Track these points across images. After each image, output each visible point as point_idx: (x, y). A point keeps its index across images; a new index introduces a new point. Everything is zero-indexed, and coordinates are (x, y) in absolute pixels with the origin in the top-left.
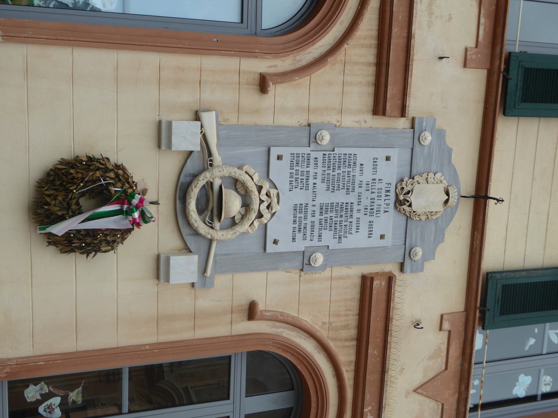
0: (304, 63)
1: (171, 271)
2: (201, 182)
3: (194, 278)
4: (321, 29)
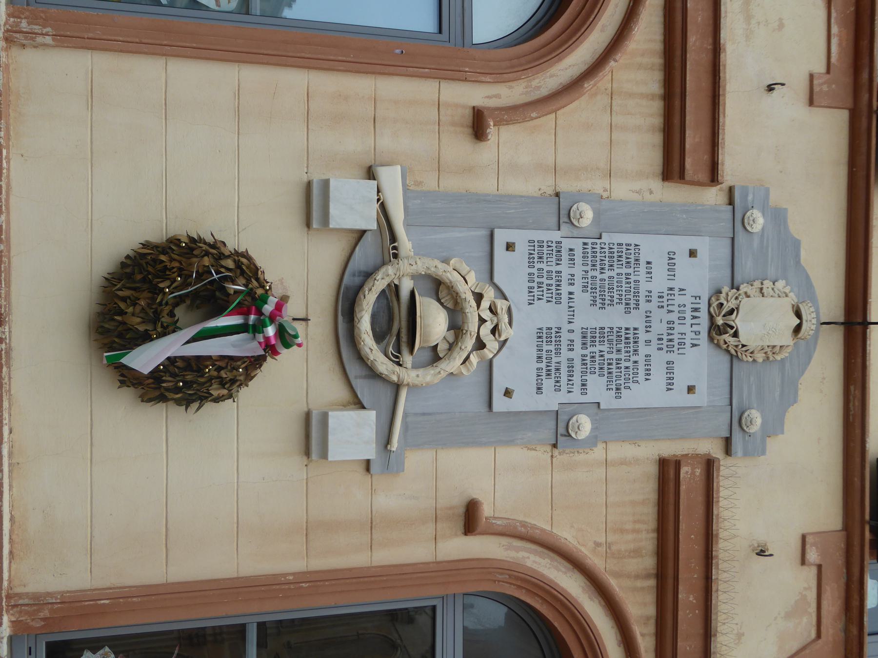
0: (544, 92)
1: (330, 437)
2: (380, 283)
3: (370, 452)
4: (570, 38)
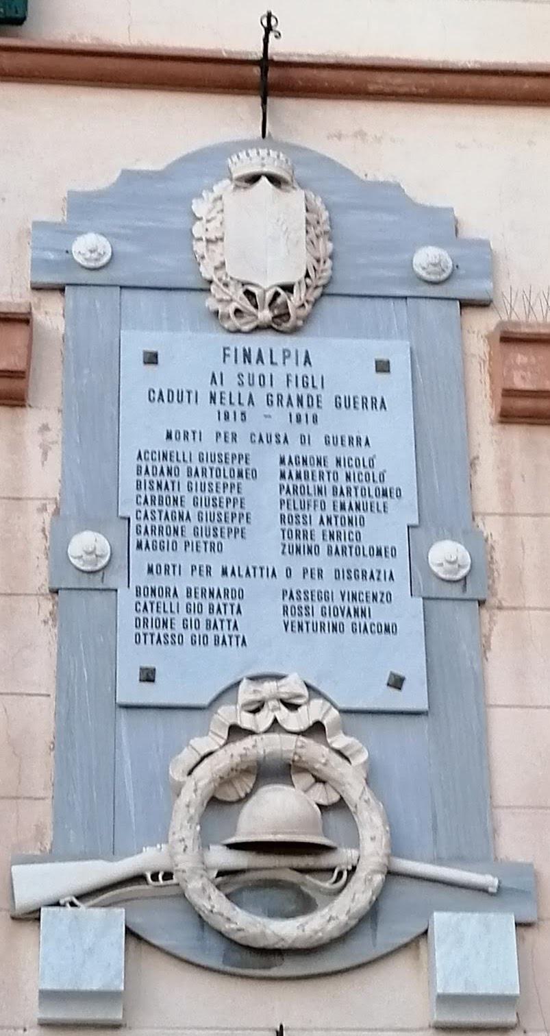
1: (481, 991)
2: (215, 903)
